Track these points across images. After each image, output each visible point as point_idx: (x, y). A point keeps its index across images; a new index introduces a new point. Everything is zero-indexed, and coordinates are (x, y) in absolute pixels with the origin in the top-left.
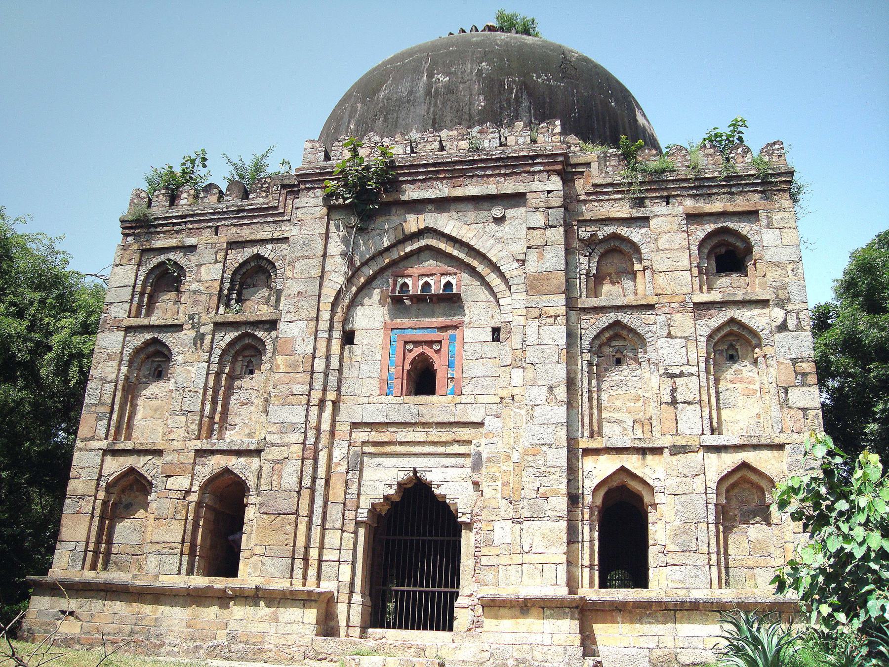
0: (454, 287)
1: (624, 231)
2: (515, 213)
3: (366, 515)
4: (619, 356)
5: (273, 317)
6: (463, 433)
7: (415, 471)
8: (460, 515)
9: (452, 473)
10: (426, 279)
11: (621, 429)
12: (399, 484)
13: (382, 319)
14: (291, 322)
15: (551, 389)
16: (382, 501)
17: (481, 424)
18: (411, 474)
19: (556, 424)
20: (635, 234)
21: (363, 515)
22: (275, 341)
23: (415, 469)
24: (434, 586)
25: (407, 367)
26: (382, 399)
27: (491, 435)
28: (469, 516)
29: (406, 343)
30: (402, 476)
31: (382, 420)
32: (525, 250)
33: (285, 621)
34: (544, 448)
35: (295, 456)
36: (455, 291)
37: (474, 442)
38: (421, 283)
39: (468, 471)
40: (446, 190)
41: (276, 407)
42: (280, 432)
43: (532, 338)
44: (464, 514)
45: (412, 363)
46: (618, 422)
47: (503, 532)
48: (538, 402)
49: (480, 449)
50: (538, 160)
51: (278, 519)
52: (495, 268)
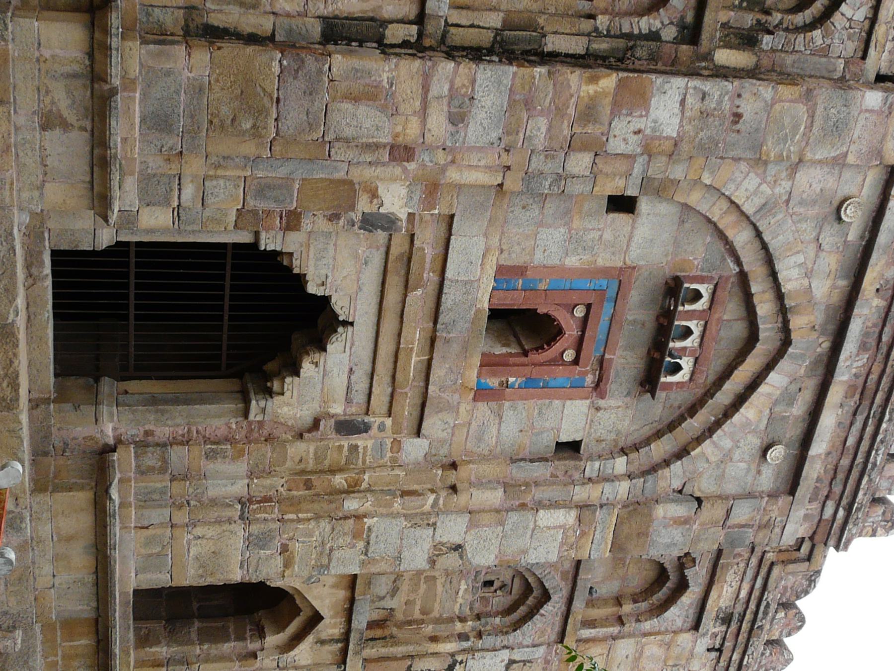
0: (670, 379)
1: (689, 599)
2: (768, 477)
3: (270, 248)
4: (497, 584)
5: (705, 36)
6: (407, 408)
7: (347, 324)
8: (262, 403)
9: (339, 382)
10: (697, 330)
11: (383, 593)
12: (325, 301)
13: (642, 263)
14: (683, 102)
15: (458, 548)
16: (296, 271)
17: (418, 433)
18: (341, 318)
19: (399, 558)
20: (679, 613)
21: (269, 242)
22: (654, 36)
23: (352, 324)
24: (137, 297)
25: (542, 310)
26: (491, 271)
27: (395, 449)
28: (259, 418)
29: (589, 307)
30: (339, 305)
31: (449, 274)
32: (697, 494)
33: (47, 145)
34: (361, 545)
35: (399, 129)
36: (663, 379)
37: (389, 422)
38: (692, 324)
39: (338, 409)
40: (845, 378)
41: (507, 81)
42: (453, 93)
43: (546, 518)
44: (264, 410)
45: (547, 316)
46: (394, 591)
47: (228, 479)
48: (439, 531)
49: (374, 431)
50: (841, 513)
51: (266, 100)
52: (682, 453)
